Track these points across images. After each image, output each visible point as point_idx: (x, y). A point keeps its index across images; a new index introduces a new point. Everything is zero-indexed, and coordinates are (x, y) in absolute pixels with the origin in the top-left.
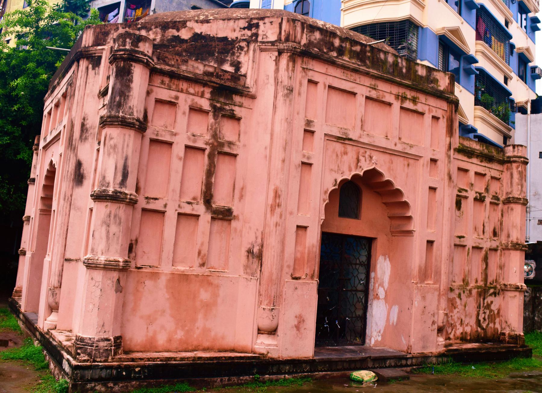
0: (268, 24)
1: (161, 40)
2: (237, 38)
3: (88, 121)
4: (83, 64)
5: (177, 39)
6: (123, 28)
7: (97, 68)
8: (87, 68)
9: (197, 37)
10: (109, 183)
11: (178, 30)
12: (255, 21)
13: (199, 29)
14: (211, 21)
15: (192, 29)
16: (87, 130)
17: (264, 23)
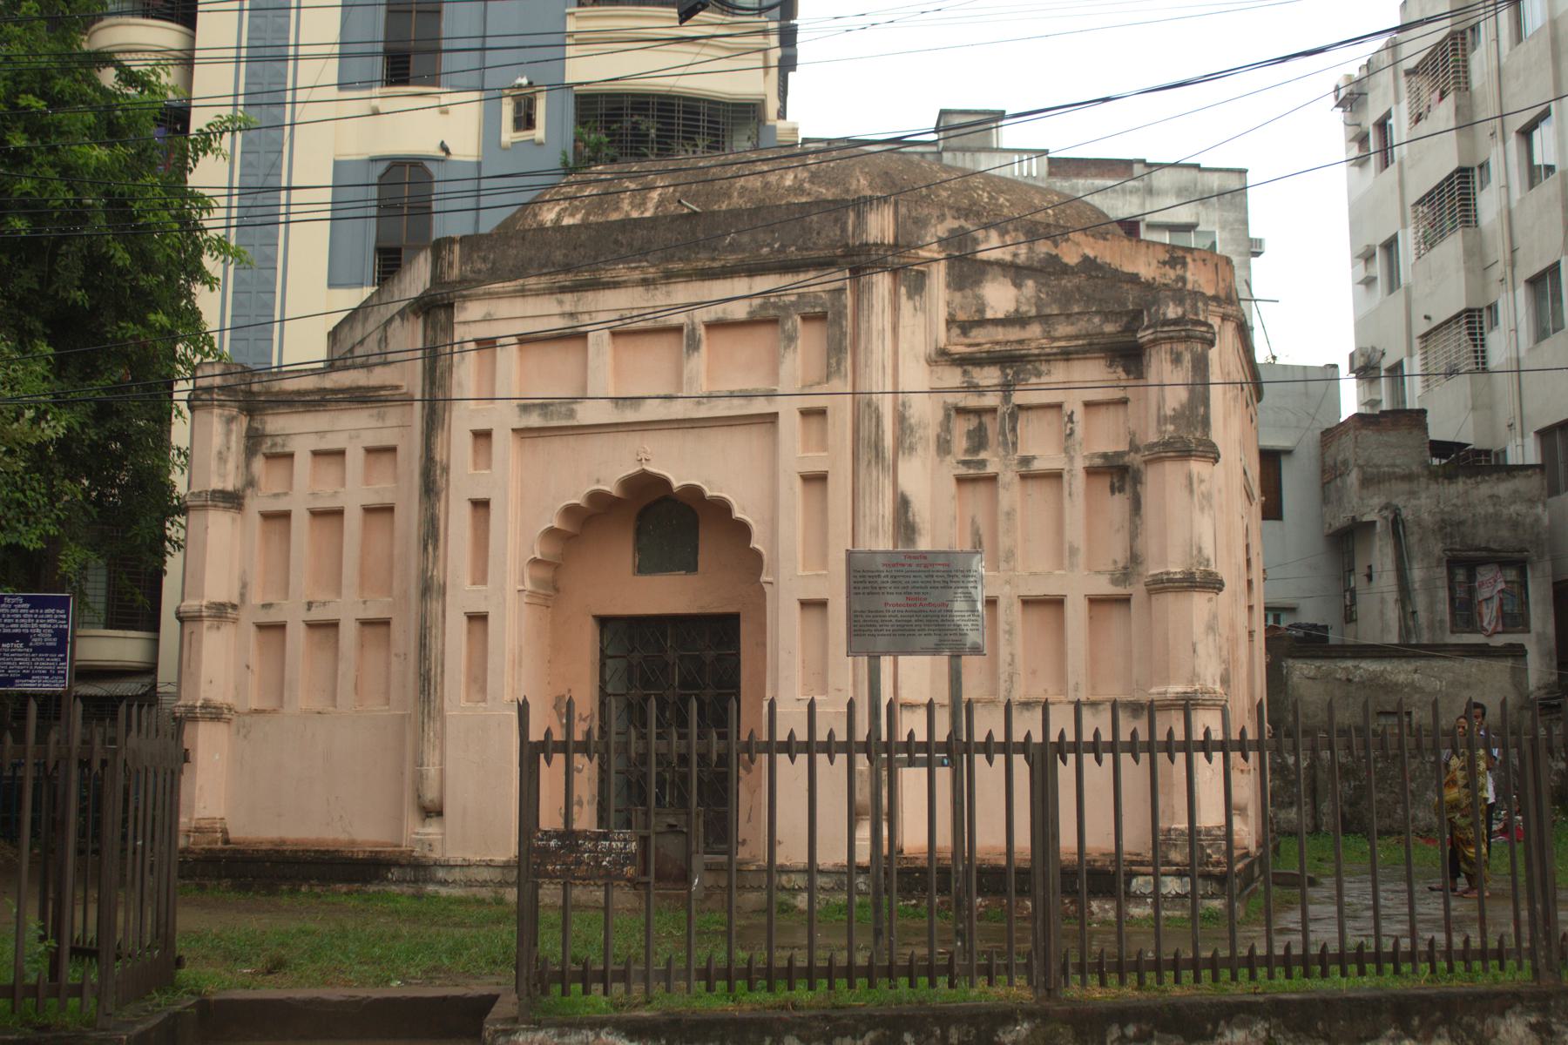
0: (1200, 263)
1: (1028, 259)
2: (1154, 279)
3: (912, 411)
4: (882, 283)
5: (1053, 260)
6: (954, 218)
7: (917, 298)
8: (895, 294)
9: (1089, 264)
10: (1208, 560)
11: (1056, 246)
12: (1180, 253)
13: (1091, 248)
14: (1109, 237)
15: (1078, 244)
16: (912, 431)
17: (1194, 260)
